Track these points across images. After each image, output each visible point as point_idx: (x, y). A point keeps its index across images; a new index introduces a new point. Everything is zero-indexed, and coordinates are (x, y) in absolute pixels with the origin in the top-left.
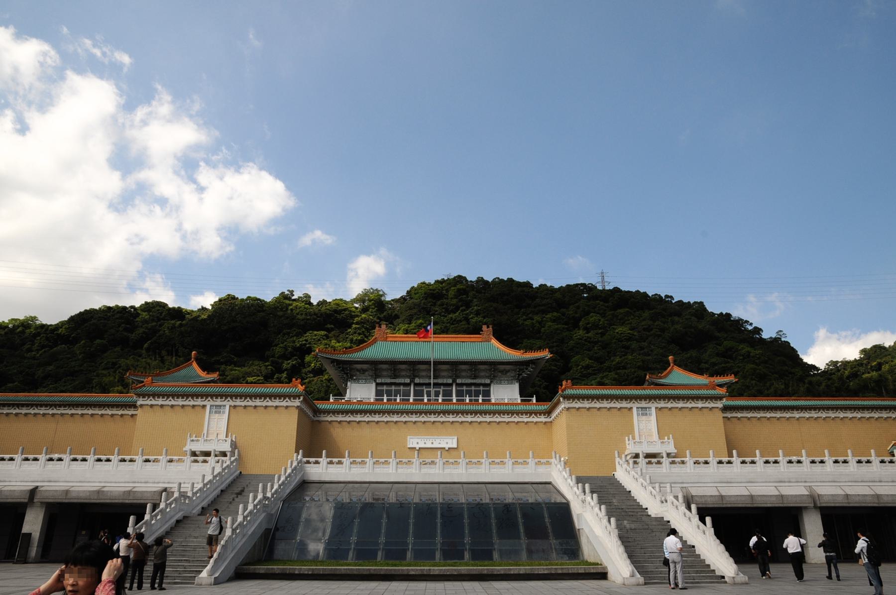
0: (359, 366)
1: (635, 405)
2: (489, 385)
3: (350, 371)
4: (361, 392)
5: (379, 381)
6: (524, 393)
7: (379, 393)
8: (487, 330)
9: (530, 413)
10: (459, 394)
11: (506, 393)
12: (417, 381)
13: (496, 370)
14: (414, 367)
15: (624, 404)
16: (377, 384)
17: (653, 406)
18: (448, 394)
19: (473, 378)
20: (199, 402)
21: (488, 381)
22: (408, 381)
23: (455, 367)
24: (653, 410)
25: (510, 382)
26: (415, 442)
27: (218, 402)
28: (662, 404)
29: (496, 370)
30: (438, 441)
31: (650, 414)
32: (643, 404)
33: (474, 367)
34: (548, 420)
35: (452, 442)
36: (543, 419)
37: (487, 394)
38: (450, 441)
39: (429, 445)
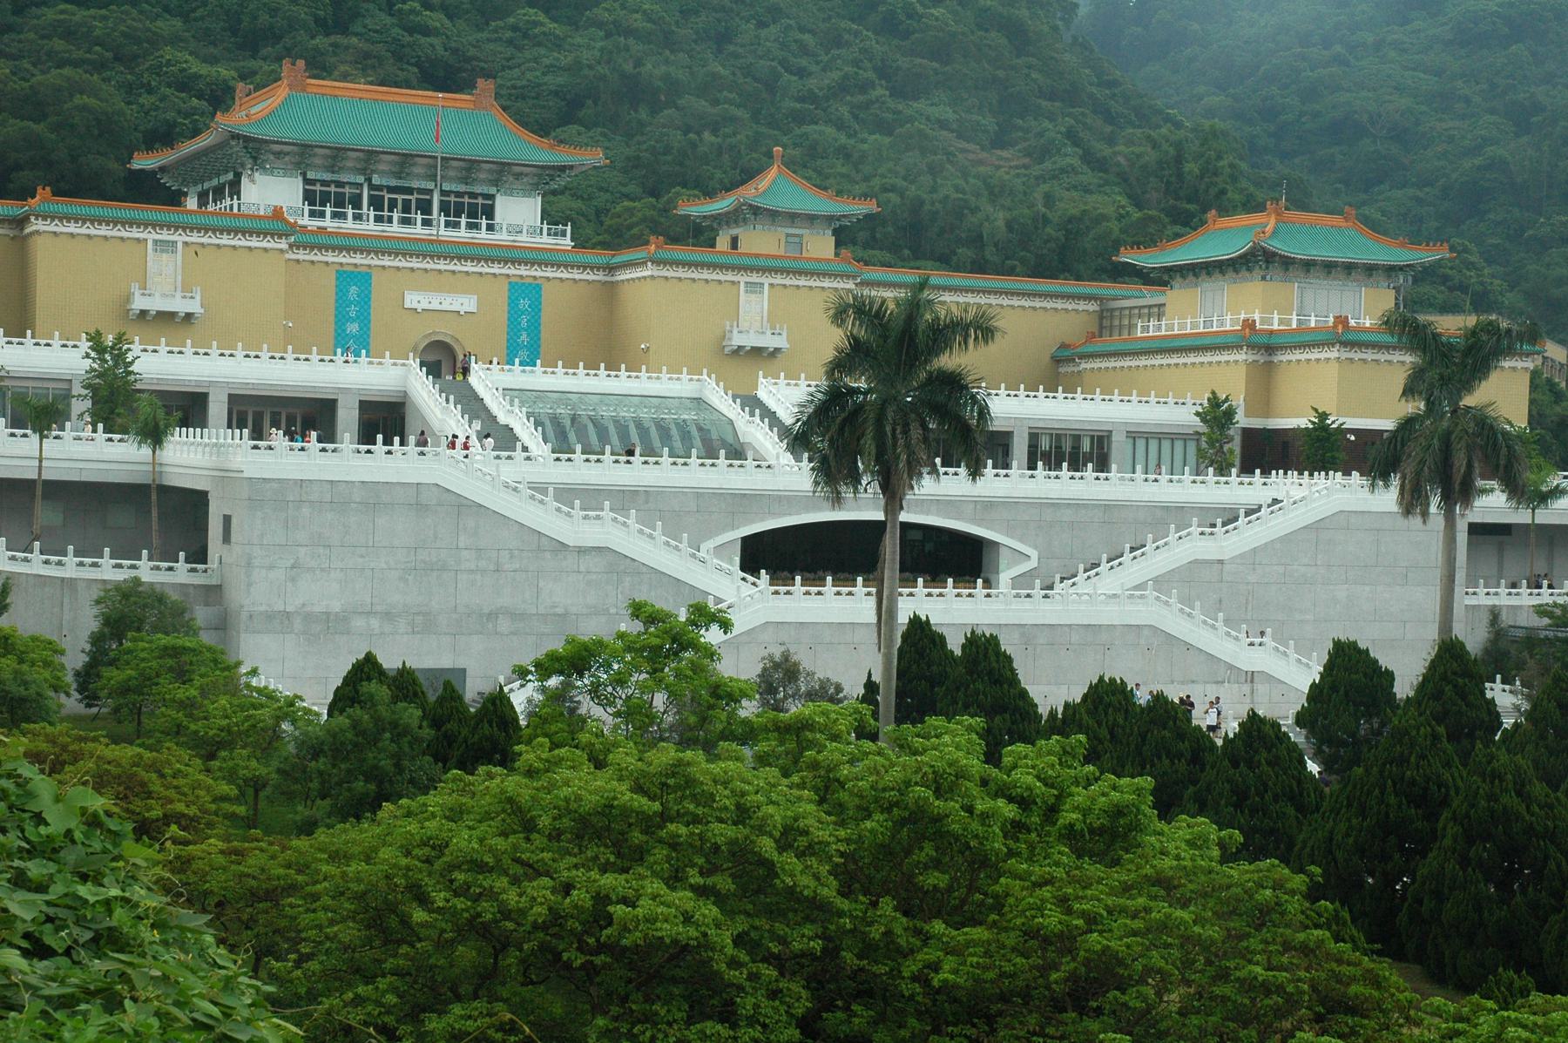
0: (276, 148)
1: (743, 278)
2: (492, 197)
3: (257, 152)
5: (310, 175)
9: (584, 267)
12: (376, 180)
13: (504, 174)
15: (730, 276)
16: (307, 181)
17: (767, 280)
20: (135, 233)
21: (493, 190)
22: (360, 179)
24: (766, 287)
25: (527, 193)
27: (165, 235)
28: (779, 280)
29: (504, 174)
30: (449, 300)
31: (761, 292)
32: (754, 278)
33: (470, 167)
34: (608, 279)
36: (600, 276)
38: (466, 301)
39: (435, 306)
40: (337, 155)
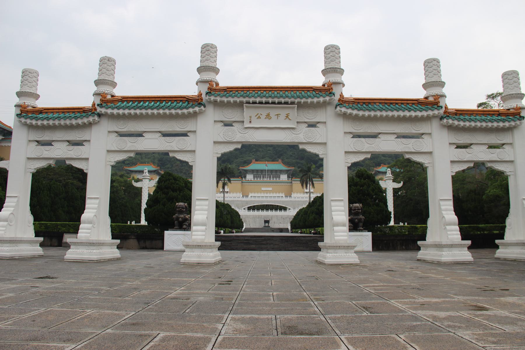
4: (250, 177)
6: (288, 177)
7: (254, 177)
8: (280, 160)
10: (273, 177)
11: (284, 177)
13: (281, 172)
14: (262, 171)
18: (270, 177)
19: (276, 173)
23: (272, 171)
26: (263, 189)
29: (281, 172)
33: (276, 171)
35: (270, 189)
37: (279, 177)
40: (257, 171)
